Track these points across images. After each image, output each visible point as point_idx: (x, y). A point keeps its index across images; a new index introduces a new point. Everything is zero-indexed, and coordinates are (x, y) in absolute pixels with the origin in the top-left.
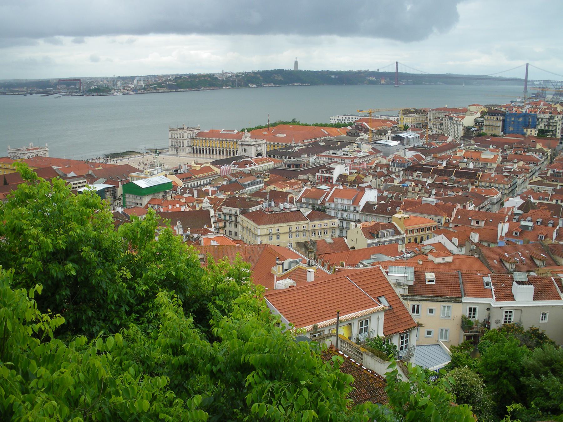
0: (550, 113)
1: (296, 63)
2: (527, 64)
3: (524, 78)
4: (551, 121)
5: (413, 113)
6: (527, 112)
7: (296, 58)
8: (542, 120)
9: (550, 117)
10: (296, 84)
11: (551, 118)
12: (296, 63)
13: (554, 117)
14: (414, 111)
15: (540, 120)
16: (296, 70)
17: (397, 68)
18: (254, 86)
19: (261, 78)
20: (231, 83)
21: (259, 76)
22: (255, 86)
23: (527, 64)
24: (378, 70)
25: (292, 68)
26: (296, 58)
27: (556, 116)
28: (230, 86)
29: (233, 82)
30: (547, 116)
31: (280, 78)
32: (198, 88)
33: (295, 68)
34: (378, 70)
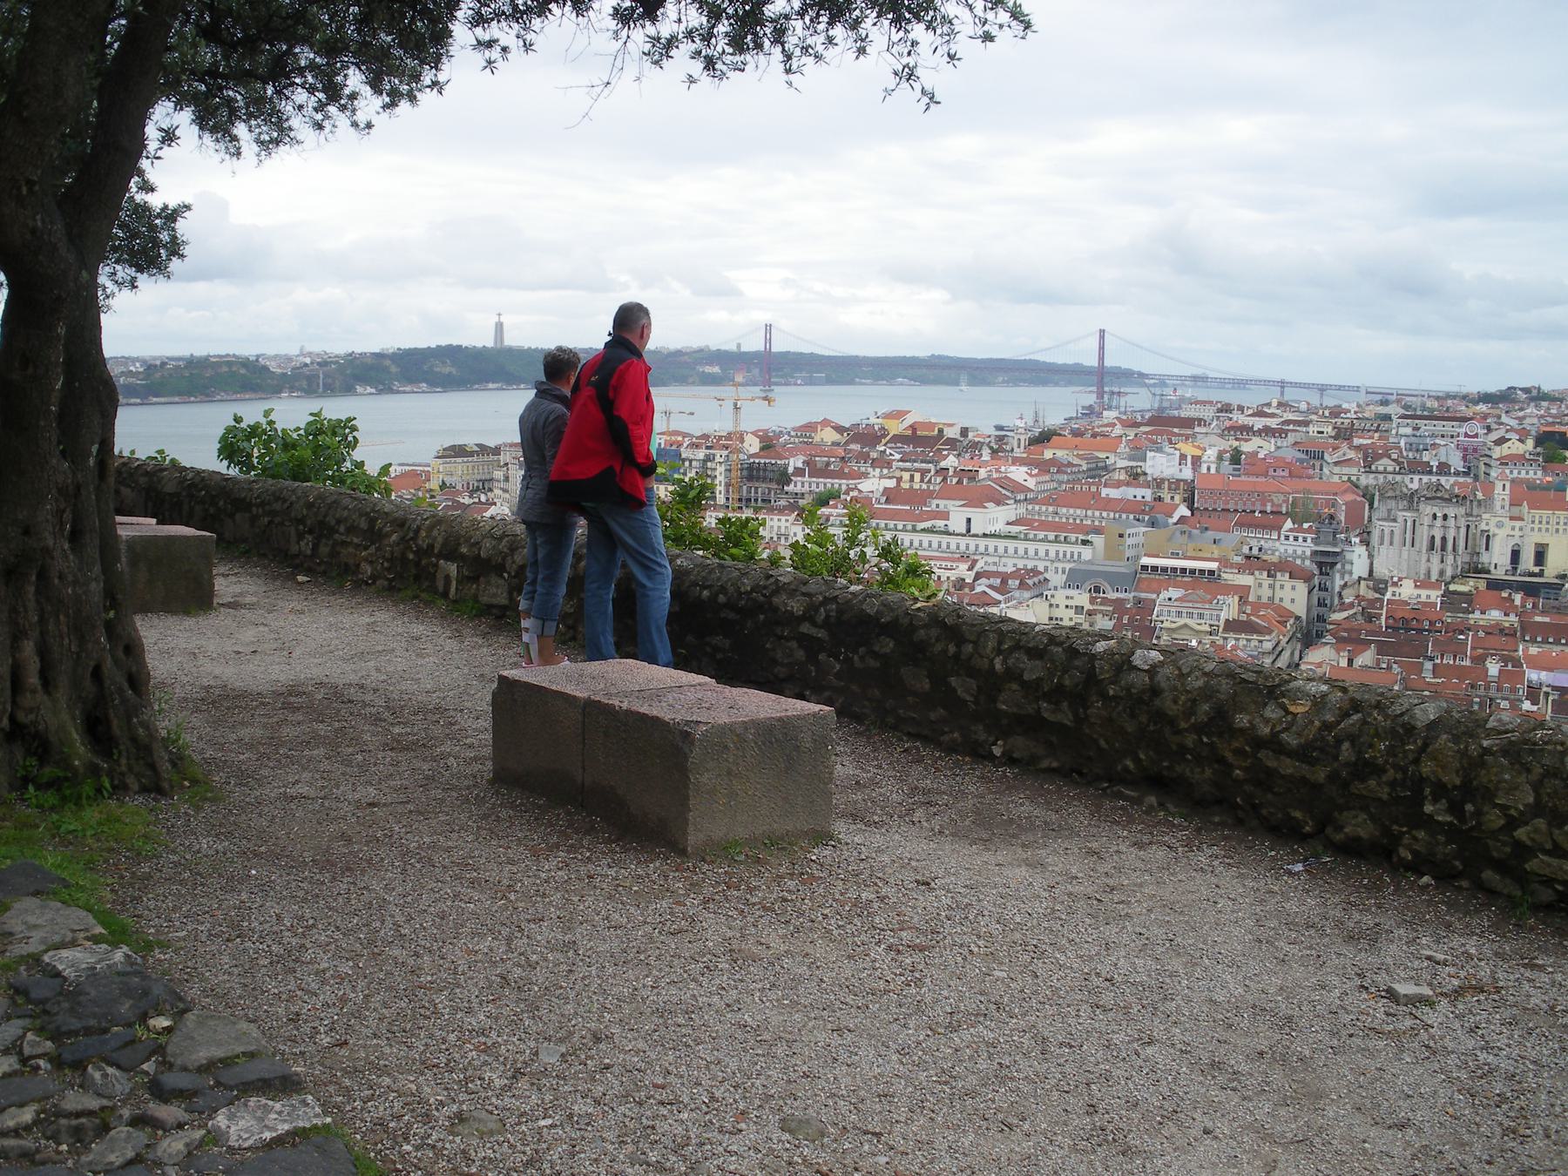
0: (707, 448)
1: (499, 327)
2: (1102, 332)
3: (1094, 362)
4: (709, 464)
5: (471, 454)
6: (662, 446)
7: (499, 315)
8: (690, 465)
9: (706, 455)
10: (491, 386)
11: (708, 458)
12: (499, 327)
13: (714, 455)
14: (476, 449)
15: (687, 464)
16: (499, 346)
17: (768, 340)
18: (369, 390)
19: (394, 369)
20: (304, 384)
21: (387, 362)
22: (373, 391)
23: (1102, 332)
24: (739, 346)
25: (490, 344)
26: (499, 315)
27: (718, 453)
28: (302, 390)
29: (312, 379)
30: (701, 454)
31: (447, 370)
32: (207, 395)
33: (496, 342)
34: (739, 346)
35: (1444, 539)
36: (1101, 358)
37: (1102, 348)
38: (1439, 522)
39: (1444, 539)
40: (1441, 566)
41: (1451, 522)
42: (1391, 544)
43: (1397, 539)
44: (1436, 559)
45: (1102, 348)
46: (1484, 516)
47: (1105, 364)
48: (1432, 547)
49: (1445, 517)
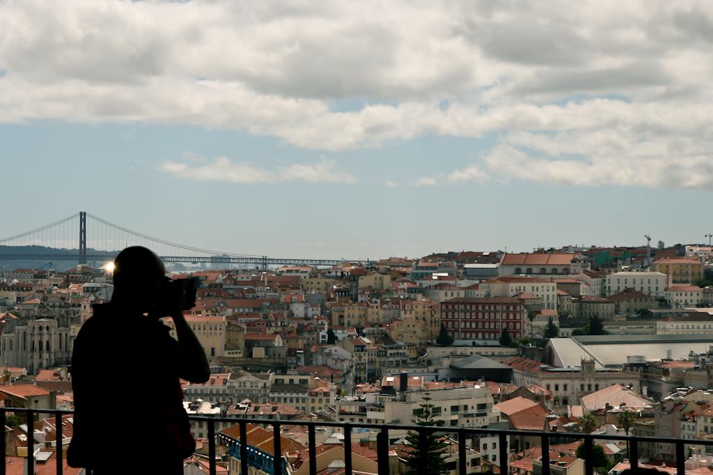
2: (83, 216)
23: (83, 216)
35: (41, 343)
36: (83, 242)
37: (83, 231)
38: (36, 331)
39: (41, 343)
40: (40, 361)
41: (45, 331)
42: (11, 348)
43: (14, 347)
44: (36, 356)
45: (83, 231)
46: (72, 327)
47: (87, 247)
48: (33, 349)
49: (41, 328)
